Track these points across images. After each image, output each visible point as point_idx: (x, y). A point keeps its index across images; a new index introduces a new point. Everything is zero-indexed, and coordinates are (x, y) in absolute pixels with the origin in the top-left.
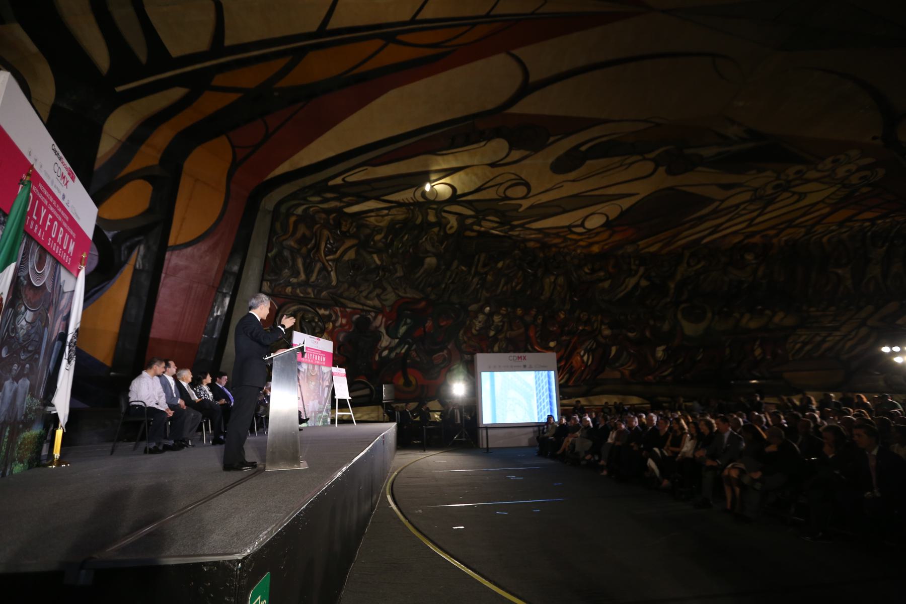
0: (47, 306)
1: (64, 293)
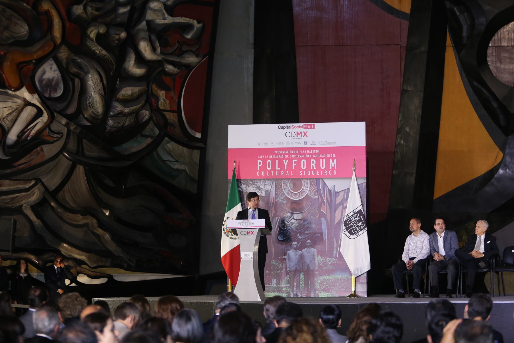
0: (317, 206)
1: (336, 193)
